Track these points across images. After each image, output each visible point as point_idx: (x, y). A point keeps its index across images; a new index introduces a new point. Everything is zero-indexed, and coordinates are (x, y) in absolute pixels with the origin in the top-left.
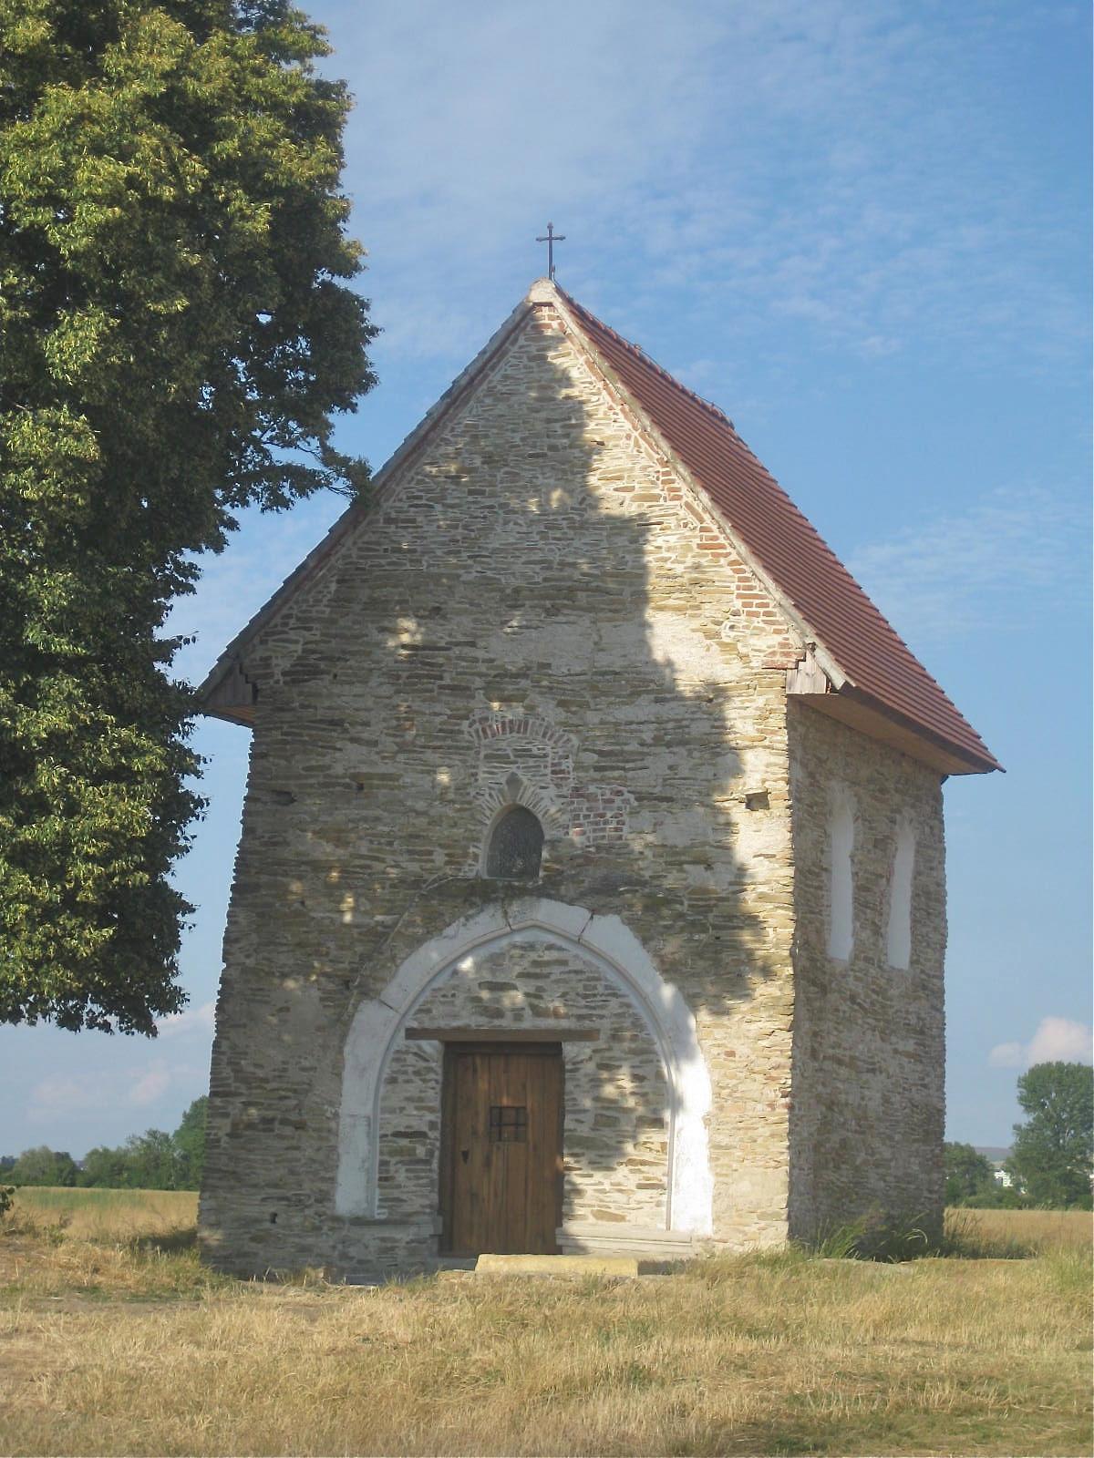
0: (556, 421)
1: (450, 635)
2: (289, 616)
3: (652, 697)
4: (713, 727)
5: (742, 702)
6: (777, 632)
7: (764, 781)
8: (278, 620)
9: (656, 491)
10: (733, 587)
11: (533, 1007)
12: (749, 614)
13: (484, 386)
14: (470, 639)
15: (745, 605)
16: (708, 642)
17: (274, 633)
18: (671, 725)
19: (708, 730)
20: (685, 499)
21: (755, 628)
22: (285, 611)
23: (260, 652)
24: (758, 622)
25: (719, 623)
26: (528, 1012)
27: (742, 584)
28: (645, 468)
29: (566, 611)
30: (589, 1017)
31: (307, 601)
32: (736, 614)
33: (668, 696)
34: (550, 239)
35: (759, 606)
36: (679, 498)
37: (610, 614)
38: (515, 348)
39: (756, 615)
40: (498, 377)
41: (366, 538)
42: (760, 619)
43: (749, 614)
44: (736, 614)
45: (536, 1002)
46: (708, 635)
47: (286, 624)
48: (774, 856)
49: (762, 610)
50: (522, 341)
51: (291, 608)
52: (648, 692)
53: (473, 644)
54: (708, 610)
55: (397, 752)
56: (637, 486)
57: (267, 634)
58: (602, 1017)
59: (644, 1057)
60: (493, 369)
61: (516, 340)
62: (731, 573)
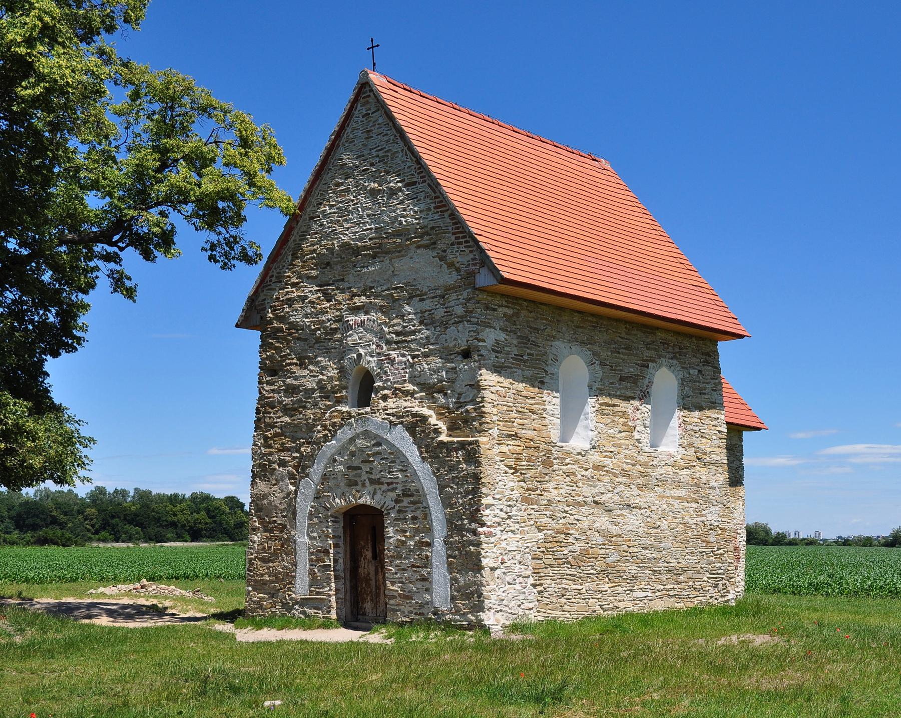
0: (373, 149)
1: (334, 277)
2: (272, 276)
3: (418, 299)
4: (446, 312)
5: (457, 296)
6: (471, 252)
7: (467, 342)
8: (268, 279)
9: (415, 180)
10: (450, 228)
11: (369, 479)
12: (458, 243)
13: (345, 136)
14: (342, 278)
15: (457, 238)
16: (441, 263)
17: (266, 286)
18: (427, 313)
19: (443, 314)
20: (427, 181)
21: (461, 251)
22: (270, 274)
23: (262, 297)
24: (462, 247)
25: (444, 251)
26: (367, 482)
27: (454, 227)
28: (409, 167)
29: (379, 255)
30: (392, 483)
31: (279, 267)
32: (452, 244)
33: (425, 297)
34: (373, 47)
35: (463, 237)
36: (425, 181)
37: (397, 254)
38: (357, 112)
39: (461, 243)
40: (350, 130)
41: (302, 230)
42: (463, 246)
43: (459, 243)
44: (452, 244)
45: (371, 476)
46: (442, 259)
47: (271, 281)
48: (474, 385)
49: (463, 240)
50: (359, 107)
51: (273, 272)
52: (416, 296)
53: (343, 280)
54: (441, 245)
55: (314, 344)
56: (406, 178)
57: (264, 287)
58: (397, 483)
59: (417, 505)
60: (348, 126)
61: (357, 107)
62: (449, 221)
